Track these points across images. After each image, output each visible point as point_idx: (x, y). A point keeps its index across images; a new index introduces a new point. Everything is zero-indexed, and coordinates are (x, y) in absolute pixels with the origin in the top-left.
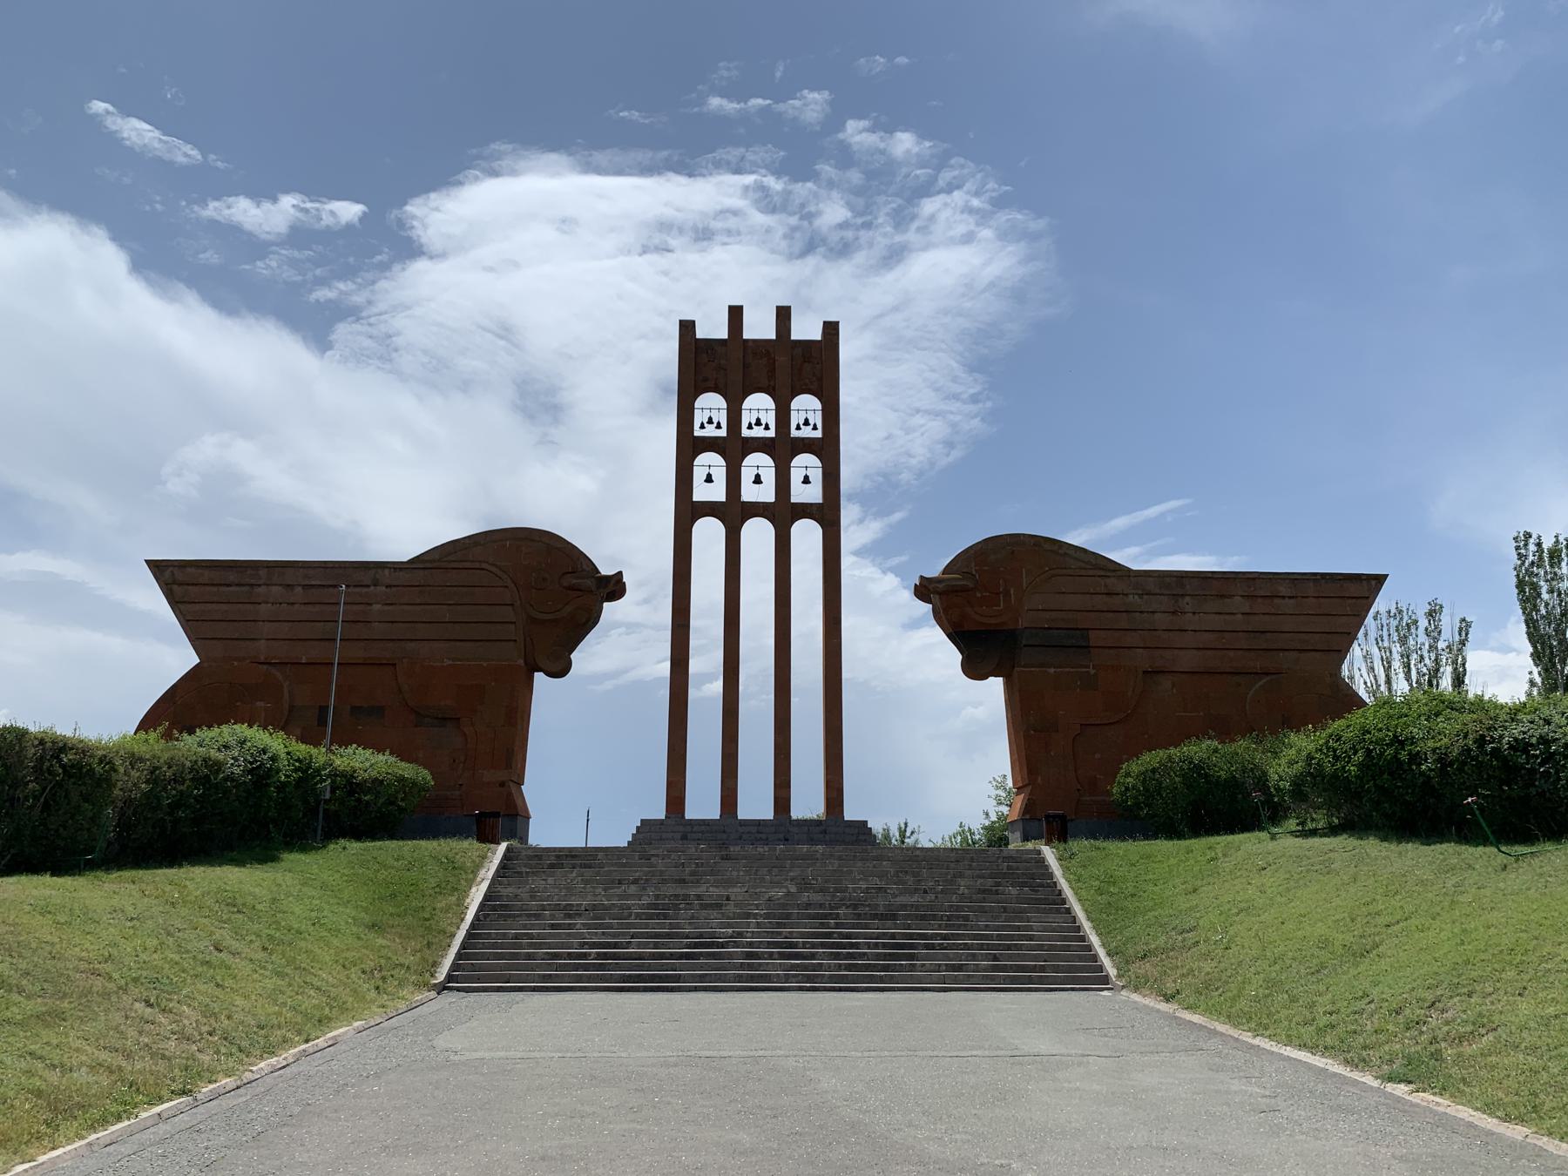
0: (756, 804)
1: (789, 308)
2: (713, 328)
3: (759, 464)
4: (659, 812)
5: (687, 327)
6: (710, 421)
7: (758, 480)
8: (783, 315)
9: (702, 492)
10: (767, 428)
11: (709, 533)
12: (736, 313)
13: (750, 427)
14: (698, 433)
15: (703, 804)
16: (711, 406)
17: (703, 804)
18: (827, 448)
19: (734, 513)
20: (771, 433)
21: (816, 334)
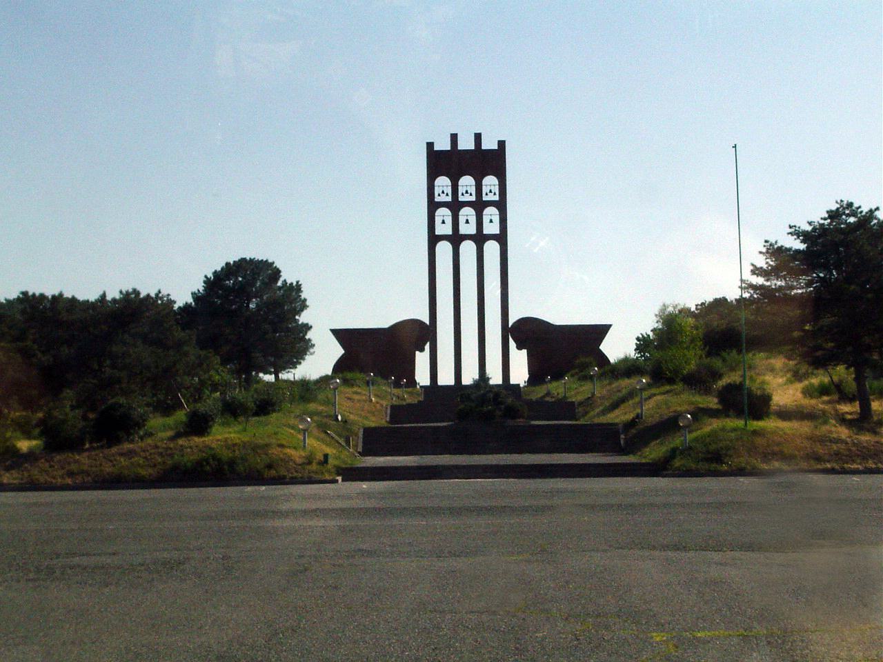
2: (443, 145)
3: (467, 213)
5: (430, 145)
7: (467, 222)
8: (478, 137)
11: (444, 249)
12: (454, 138)
14: (437, 199)
16: (443, 183)
17: (446, 378)
18: (501, 205)
19: (456, 239)
21: (496, 147)
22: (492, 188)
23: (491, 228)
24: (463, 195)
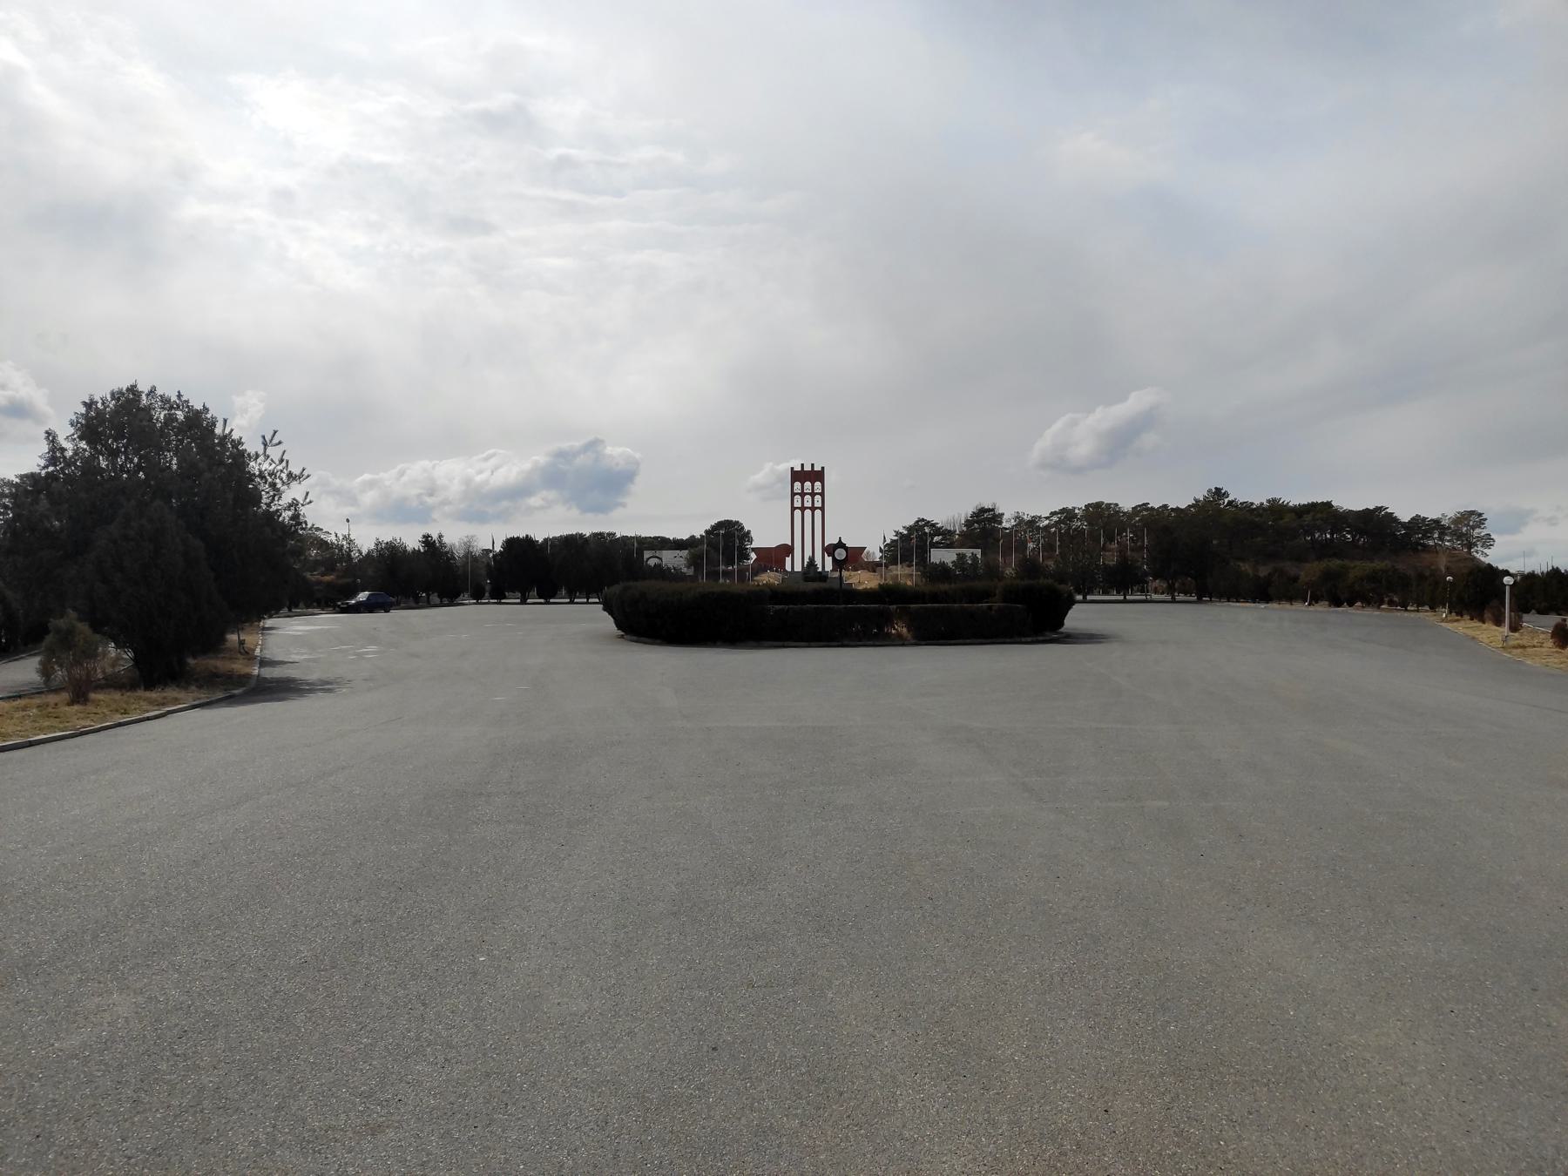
3: (807, 498)
11: (798, 513)
16: (797, 485)
18: (822, 494)
19: (803, 509)
23: (818, 504)
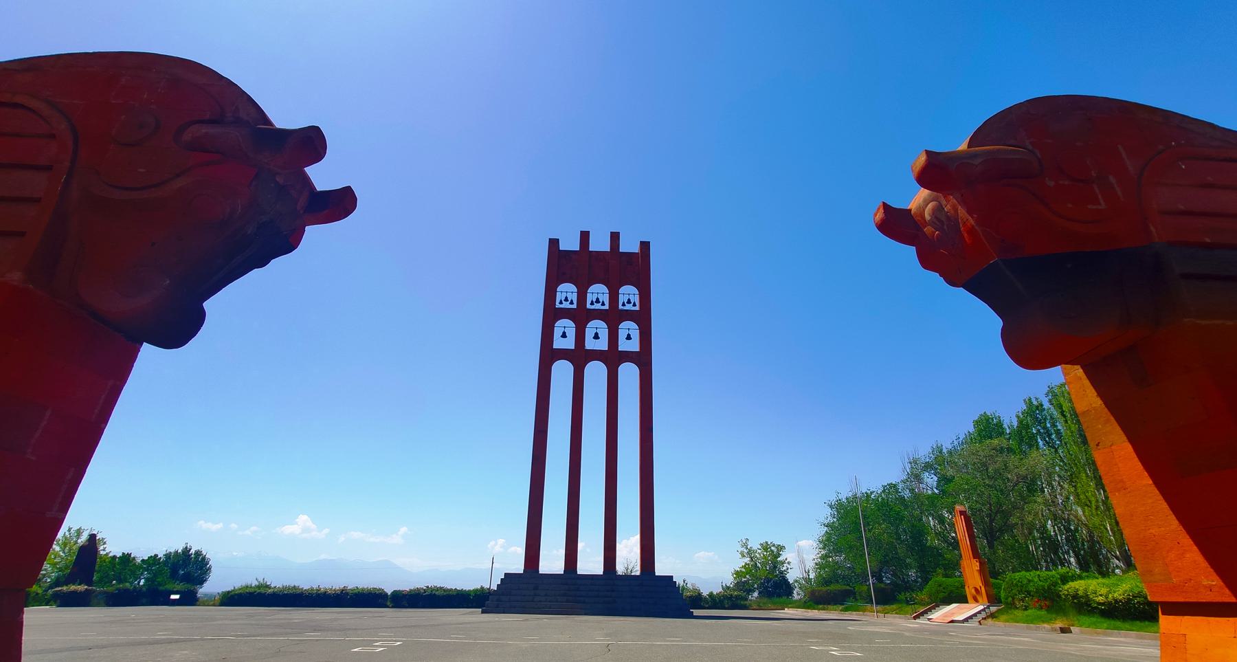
0: (590, 563)
1: (618, 233)
2: (570, 243)
4: (518, 567)
5: (554, 243)
6: (566, 299)
7: (596, 337)
8: (615, 237)
9: (559, 343)
10: (603, 304)
11: (562, 372)
12: (585, 236)
13: (592, 303)
14: (558, 305)
15: (552, 562)
16: (567, 292)
17: (552, 562)
18: (643, 318)
19: (580, 357)
20: (606, 307)
21: (636, 249)
22: (632, 298)
24: (592, 303)
